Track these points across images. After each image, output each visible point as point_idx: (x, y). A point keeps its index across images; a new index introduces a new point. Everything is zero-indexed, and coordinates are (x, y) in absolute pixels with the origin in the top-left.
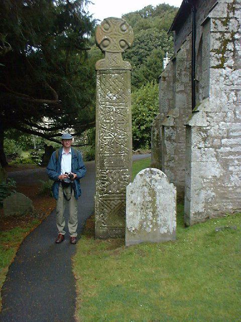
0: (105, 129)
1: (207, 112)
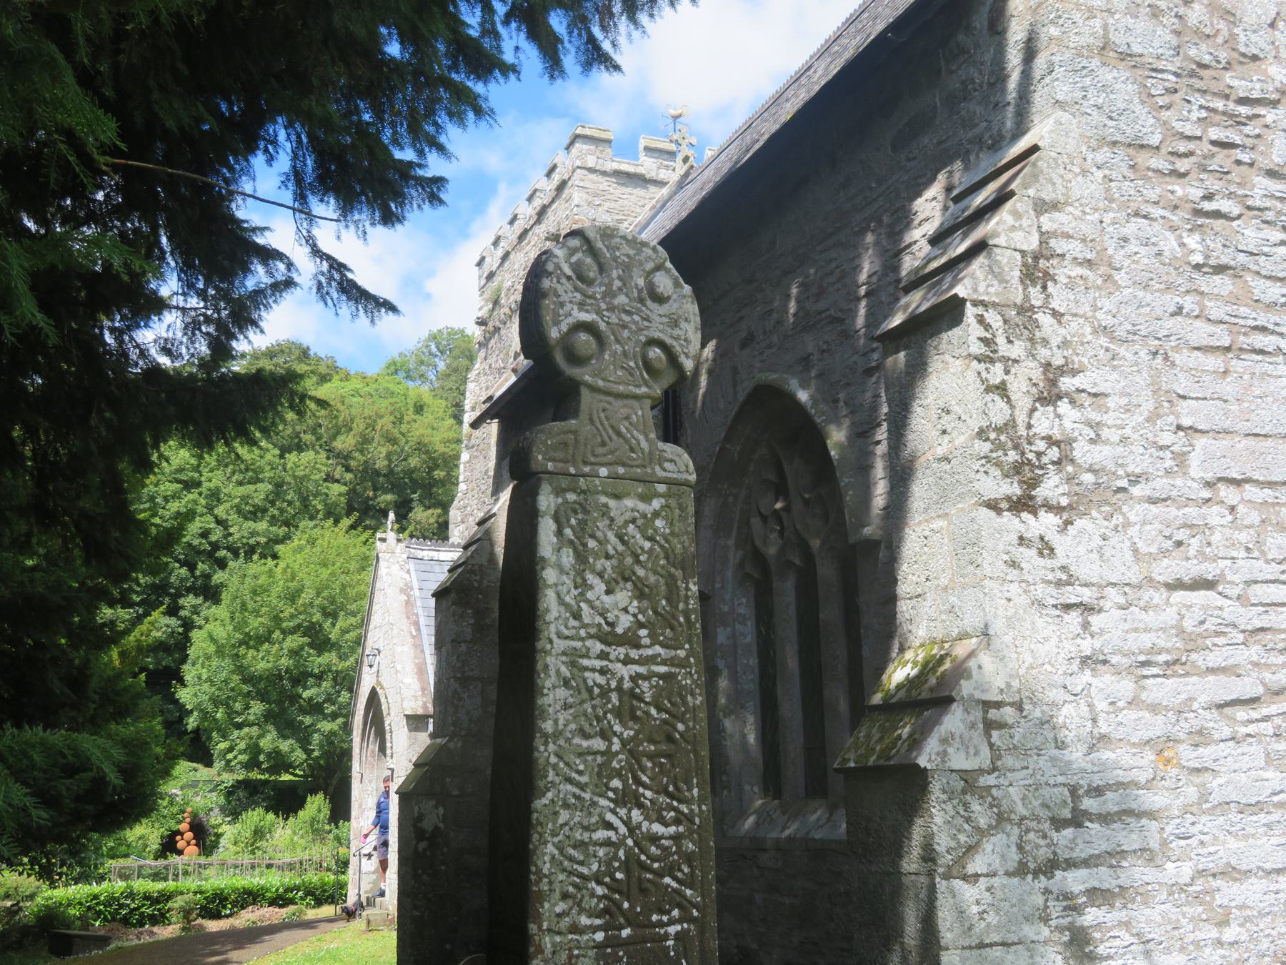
0: (582, 787)
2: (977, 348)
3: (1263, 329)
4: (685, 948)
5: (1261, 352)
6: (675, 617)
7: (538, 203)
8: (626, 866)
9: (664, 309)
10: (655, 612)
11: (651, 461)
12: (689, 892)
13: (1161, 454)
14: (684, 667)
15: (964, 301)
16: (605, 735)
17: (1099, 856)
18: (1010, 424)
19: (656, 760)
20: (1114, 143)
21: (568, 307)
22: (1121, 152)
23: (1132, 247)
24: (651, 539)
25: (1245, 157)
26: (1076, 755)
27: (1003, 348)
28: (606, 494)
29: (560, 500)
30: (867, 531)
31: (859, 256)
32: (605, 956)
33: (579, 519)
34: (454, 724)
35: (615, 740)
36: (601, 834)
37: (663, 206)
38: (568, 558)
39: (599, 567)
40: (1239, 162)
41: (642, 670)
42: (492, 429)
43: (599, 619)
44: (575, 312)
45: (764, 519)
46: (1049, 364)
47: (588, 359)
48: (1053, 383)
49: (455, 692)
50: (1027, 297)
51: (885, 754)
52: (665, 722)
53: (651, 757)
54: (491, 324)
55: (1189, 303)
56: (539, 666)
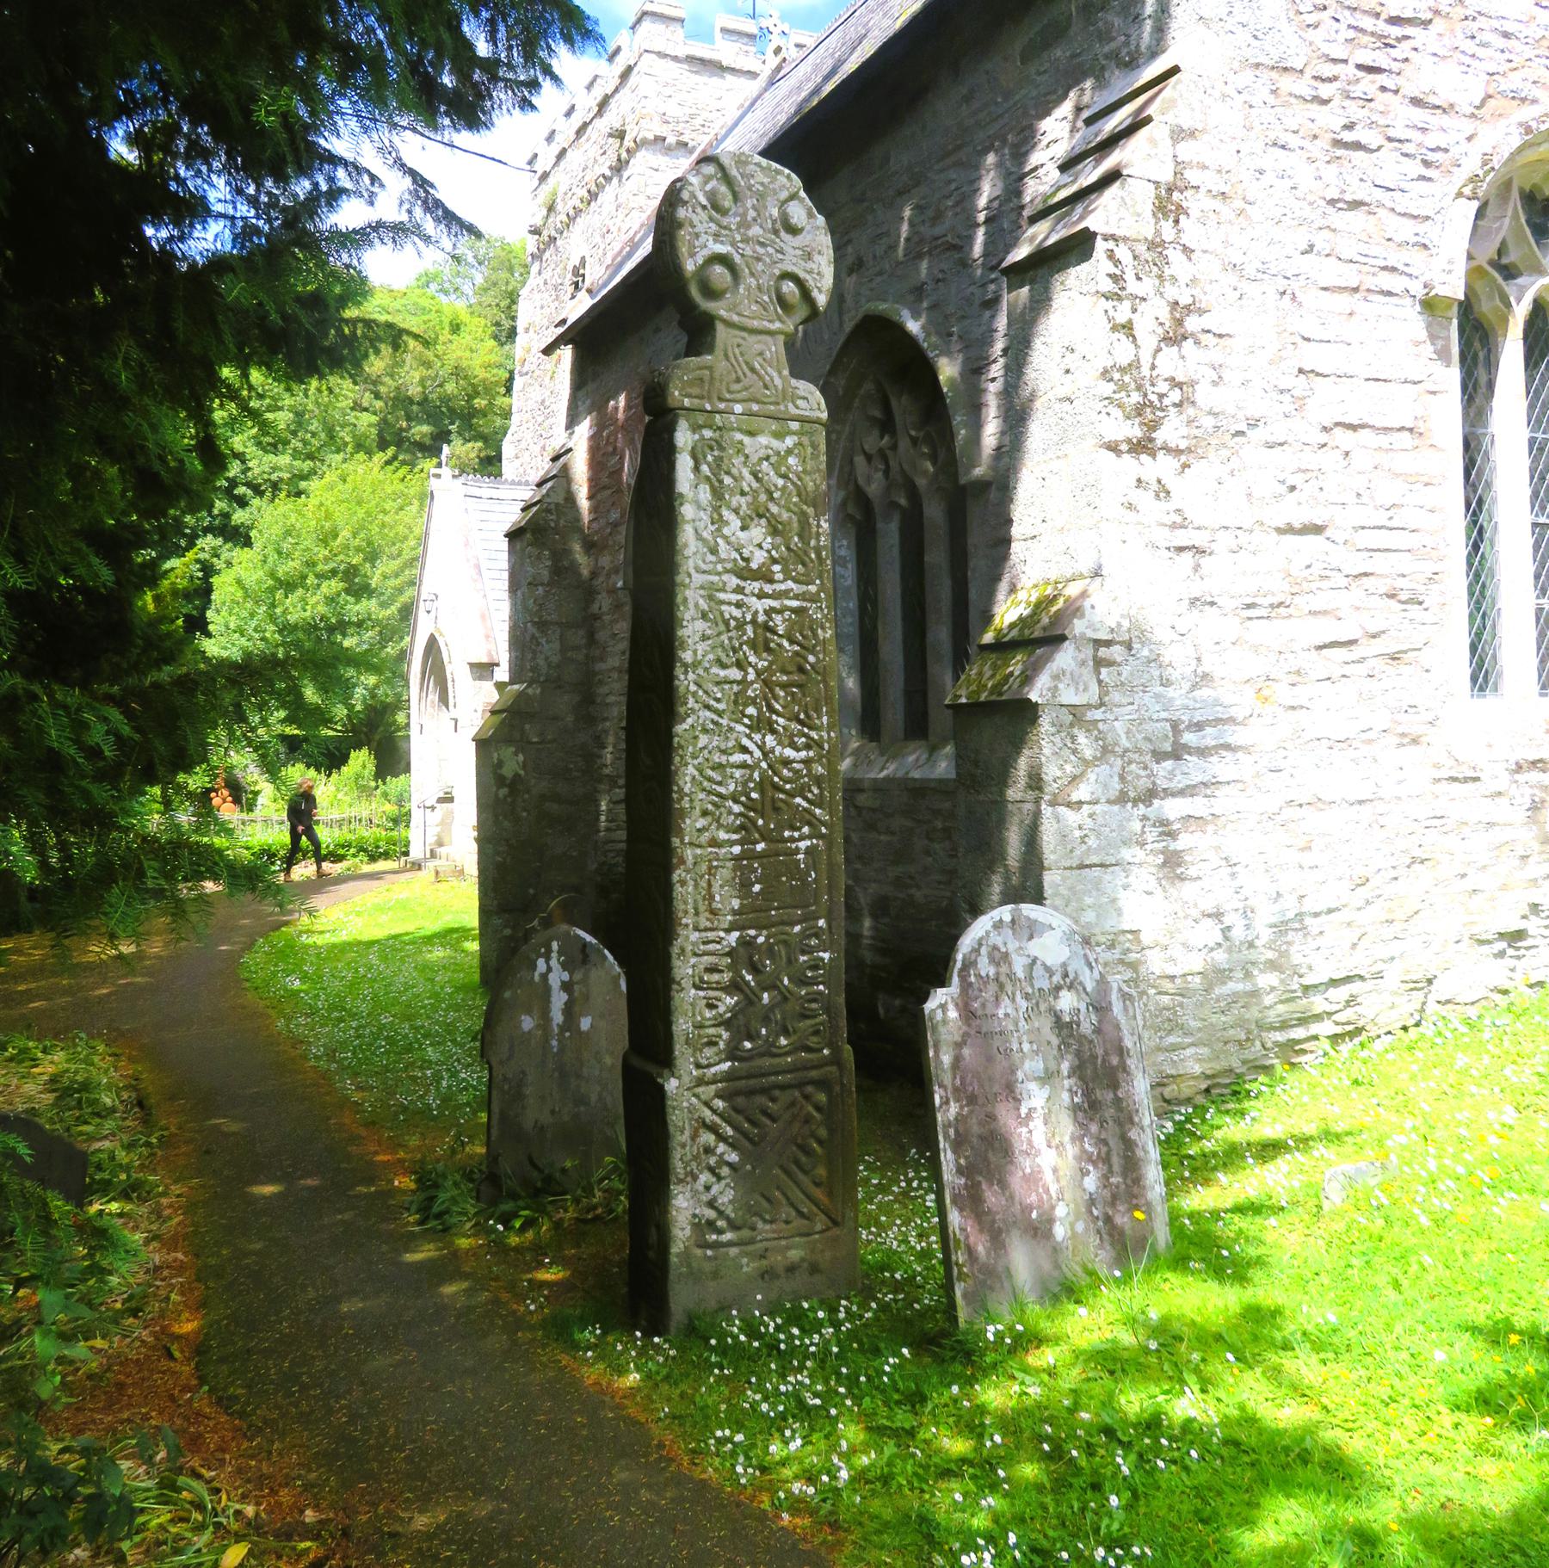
0: (720, 714)
2: (1108, 286)
3: (1394, 269)
5: (1389, 294)
6: (806, 553)
7: (599, 92)
8: (761, 787)
9: (797, 241)
10: (788, 549)
11: (784, 398)
12: (818, 811)
13: (1281, 398)
15: (1095, 234)
16: (739, 665)
17: (1194, 786)
18: (1135, 365)
20: (1257, 65)
21: (703, 238)
22: (1266, 75)
23: (1269, 178)
24: (784, 476)
25: (1391, 85)
26: (1176, 694)
27: (1132, 286)
28: (740, 430)
29: (697, 437)
30: (978, 472)
31: (979, 178)
32: (741, 868)
33: (714, 454)
34: (533, 670)
35: (750, 670)
36: (738, 758)
37: (752, 104)
38: (705, 494)
39: (734, 504)
40: (1383, 89)
41: (775, 604)
42: (566, 353)
43: (735, 555)
44: (710, 243)
45: (869, 458)
46: (1177, 303)
47: (723, 292)
48: (1180, 322)
49: (533, 637)
50: (1158, 233)
51: (997, 689)
52: (796, 654)
53: (784, 686)
54: (545, 233)
55: (1322, 241)
56: (679, 599)
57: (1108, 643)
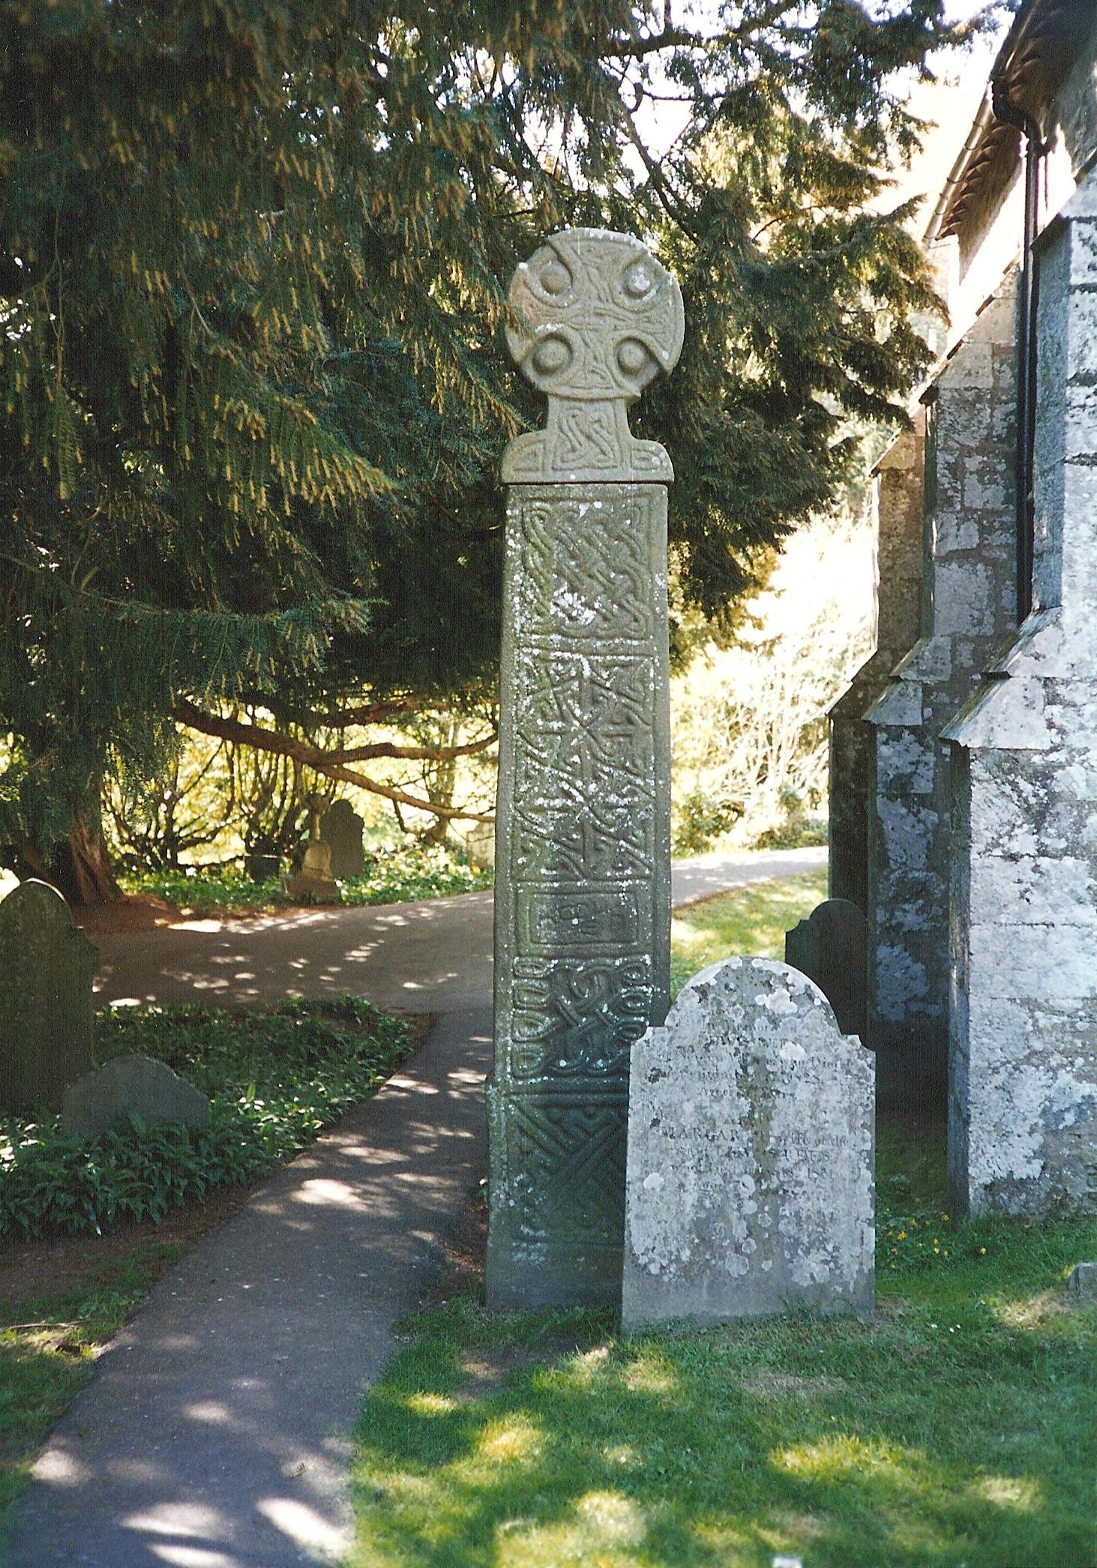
0: (542, 762)
1: (1047, 682)
4: (636, 901)
10: (621, 606)
12: (642, 855)
14: (648, 656)
19: (616, 740)
36: (558, 803)
38: (534, 560)
52: (625, 705)
57: (1066, 683)
